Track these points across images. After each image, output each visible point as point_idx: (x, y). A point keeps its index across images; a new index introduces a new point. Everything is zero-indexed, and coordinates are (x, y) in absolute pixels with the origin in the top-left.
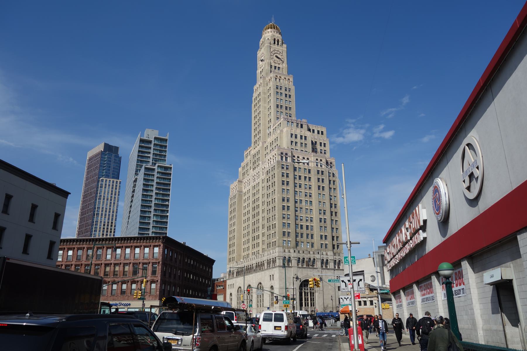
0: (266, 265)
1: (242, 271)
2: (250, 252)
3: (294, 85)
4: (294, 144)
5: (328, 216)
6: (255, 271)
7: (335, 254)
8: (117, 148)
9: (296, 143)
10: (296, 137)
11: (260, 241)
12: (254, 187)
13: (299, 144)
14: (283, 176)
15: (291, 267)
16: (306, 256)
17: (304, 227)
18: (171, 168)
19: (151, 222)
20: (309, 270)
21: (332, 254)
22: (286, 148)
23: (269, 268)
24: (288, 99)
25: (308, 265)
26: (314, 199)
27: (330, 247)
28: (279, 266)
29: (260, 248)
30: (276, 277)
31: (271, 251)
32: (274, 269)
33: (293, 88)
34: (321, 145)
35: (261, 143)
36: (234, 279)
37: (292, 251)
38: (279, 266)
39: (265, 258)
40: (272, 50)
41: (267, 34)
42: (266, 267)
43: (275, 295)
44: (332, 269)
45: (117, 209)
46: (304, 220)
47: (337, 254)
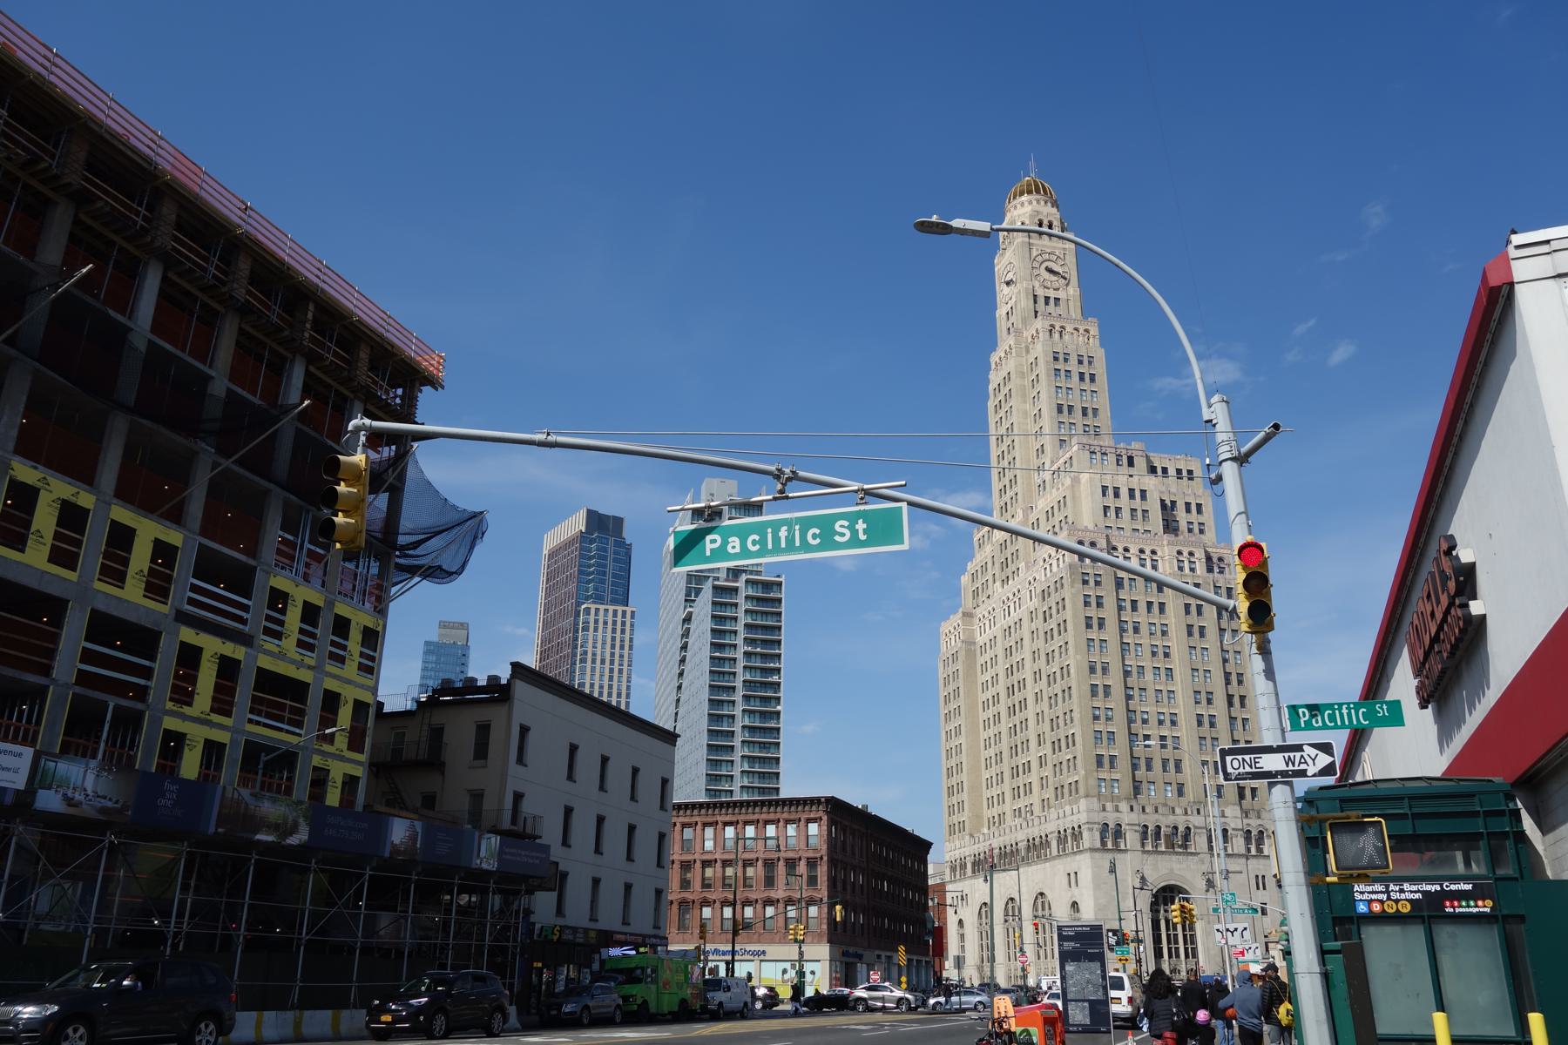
0: (1054, 844)
2: (1008, 807)
3: (1102, 345)
4: (1112, 513)
5: (1219, 708)
6: (1026, 861)
7: (1246, 814)
8: (619, 522)
9: (1118, 510)
10: (1117, 495)
11: (1034, 778)
12: (1008, 631)
13: (1126, 514)
14: (1087, 604)
15: (1125, 851)
16: (1166, 821)
18: (780, 584)
19: (737, 728)
20: (1174, 858)
22: (1091, 527)
24: (1087, 385)
25: (1171, 845)
26: (1178, 663)
28: (1092, 850)
29: (1035, 799)
30: (1086, 876)
32: (1078, 857)
33: (1099, 354)
34: (1188, 510)
35: (1020, 512)
36: (967, 882)
37: (1124, 806)
38: (1092, 850)
39: (1051, 827)
40: (1034, 253)
41: (1020, 211)
42: (1055, 852)
45: (628, 688)
46: (1153, 721)
47: (1252, 814)
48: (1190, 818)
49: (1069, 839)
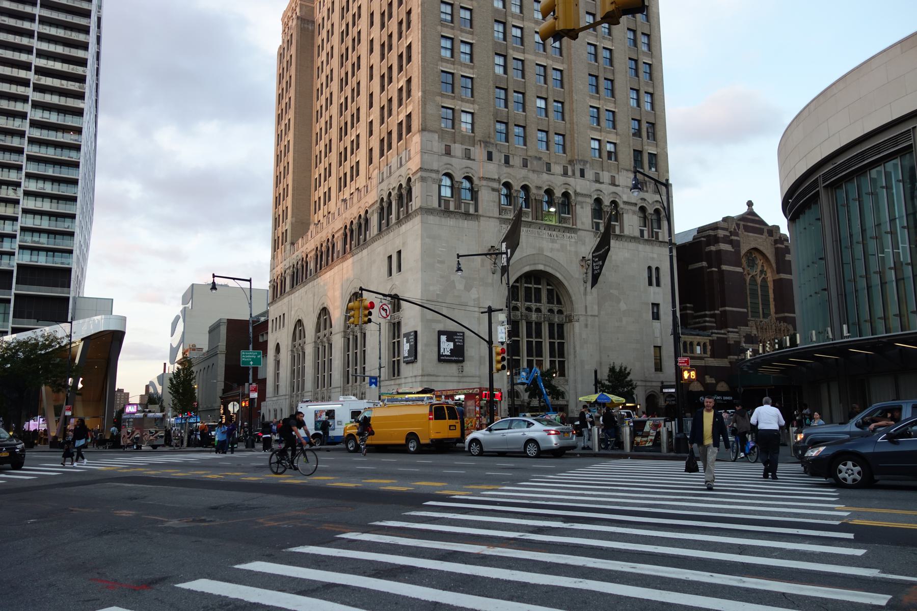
1: (304, 263)
11: (362, 155)
15: (476, 217)
16: (538, 181)
17: (531, 70)
20: (545, 233)
23: (385, 226)
27: (626, 158)
28: (426, 211)
29: (361, 181)
30: (411, 258)
36: (286, 300)
37: (479, 152)
38: (426, 211)
39: (372, 198)
43: (404, 330)
44: (632, 239)
48: (571, 181)
49: (395, 206)
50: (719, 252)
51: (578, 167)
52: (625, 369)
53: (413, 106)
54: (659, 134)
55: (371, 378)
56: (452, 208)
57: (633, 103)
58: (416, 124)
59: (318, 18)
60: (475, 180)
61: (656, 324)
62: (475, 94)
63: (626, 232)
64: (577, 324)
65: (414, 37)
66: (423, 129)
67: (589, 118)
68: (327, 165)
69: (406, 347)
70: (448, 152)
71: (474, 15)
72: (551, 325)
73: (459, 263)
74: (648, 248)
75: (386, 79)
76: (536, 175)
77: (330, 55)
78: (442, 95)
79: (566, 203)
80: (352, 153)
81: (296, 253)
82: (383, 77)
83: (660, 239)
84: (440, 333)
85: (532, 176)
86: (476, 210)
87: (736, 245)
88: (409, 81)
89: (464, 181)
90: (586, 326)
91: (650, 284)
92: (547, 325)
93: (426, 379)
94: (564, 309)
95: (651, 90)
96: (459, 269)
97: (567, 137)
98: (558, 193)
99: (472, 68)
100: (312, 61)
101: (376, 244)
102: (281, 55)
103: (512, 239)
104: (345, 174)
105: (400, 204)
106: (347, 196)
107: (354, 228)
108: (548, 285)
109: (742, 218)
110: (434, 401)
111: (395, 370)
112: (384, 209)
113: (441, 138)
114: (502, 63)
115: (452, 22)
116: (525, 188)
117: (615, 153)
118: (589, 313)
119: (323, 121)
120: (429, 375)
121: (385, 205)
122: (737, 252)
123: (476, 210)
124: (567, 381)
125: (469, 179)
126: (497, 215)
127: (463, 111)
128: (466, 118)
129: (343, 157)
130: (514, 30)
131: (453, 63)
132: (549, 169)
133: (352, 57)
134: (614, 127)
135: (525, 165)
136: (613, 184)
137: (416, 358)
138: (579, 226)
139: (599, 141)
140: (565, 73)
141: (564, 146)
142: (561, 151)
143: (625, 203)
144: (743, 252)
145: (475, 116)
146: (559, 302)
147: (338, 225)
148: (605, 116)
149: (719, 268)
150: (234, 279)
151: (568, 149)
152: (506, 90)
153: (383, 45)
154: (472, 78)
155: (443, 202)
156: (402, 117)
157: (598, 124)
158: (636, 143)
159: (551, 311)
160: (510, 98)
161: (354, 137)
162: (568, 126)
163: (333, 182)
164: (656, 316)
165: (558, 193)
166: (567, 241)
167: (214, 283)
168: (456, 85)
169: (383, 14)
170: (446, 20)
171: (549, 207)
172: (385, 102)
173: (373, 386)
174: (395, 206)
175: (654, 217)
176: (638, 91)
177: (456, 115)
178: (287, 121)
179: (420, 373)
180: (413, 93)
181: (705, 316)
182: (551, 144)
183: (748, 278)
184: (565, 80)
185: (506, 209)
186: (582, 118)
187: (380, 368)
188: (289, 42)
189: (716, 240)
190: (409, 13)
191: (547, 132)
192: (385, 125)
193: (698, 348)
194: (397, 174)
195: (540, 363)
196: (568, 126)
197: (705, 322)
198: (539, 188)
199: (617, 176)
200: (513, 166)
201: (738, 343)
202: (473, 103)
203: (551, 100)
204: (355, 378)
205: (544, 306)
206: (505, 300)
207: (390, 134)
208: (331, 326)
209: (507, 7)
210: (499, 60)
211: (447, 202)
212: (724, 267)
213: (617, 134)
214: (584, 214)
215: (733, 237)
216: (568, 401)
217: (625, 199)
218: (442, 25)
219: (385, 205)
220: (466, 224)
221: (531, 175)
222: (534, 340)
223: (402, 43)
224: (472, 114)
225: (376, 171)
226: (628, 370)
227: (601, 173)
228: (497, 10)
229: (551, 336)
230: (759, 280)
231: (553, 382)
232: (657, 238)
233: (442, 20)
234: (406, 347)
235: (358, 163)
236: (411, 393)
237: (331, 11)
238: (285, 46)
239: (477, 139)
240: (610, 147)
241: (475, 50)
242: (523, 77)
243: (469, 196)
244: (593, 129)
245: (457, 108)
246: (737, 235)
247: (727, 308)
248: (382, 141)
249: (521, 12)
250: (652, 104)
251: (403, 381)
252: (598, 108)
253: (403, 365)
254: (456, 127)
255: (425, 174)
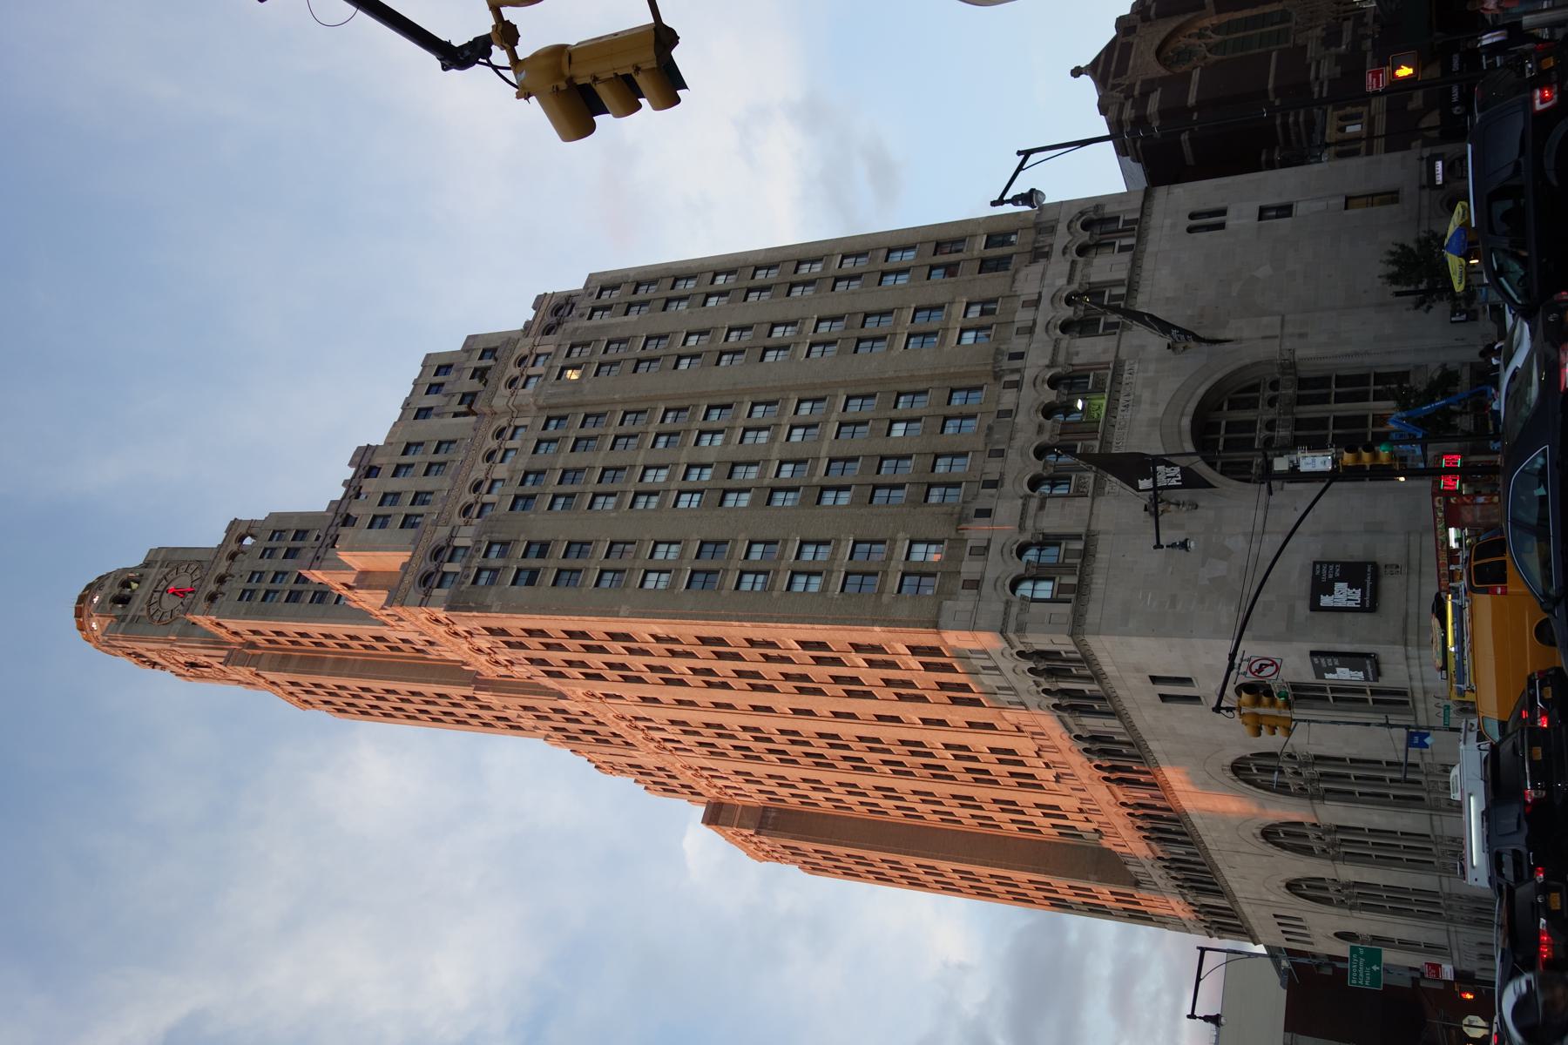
0: (1094, 724)
1: (1172, 864)
7: (1039, 254)
11: (980, 742)
15: (1089, 538)
16: (1028, 429)
17: (846, 448)
20: (1122, 415)
21: (1037, 268)
22: (404, 557)
27: (991, 285)
28: (1077, 627)
29: (1024, 746)
30: (1163, 655)
31: (990, 681)
32: (1108, 669)
36: (1247, 909)
37: (977, 532)
38: (1077, 627)
43: (1309, 677)
44: (1135, 265)
48: (1029, 374)
50: (1162, 113)
51: (1006, 364)
52: (1392, 253)
53: (897, 641)
54: (955, 233)
55: (1410, 743)
56: (1073, 580)
57: (902, 280)
58: (926, 638)
59: (759, 800)
60: (1026, 537)
61: (1300, 209)
62: (880, 537)
63: (1122, 274)
64: (1299, 353)
65: (788, 635)
66: (935, 625)
67: (924, 350)
68: (996, 807)
69: (1344, 674)
70: (974, 585)
71: (759, 538)
72: (1301, 400)
73: (1173, 546)
74: (1153, 236)
75: (853, 688)
76: (1018, 435)
77: (816, 785)
78: (881, 592)
79: (1068, 381)
80: (975, 759)
81: (1155, 879)
82: (850, 694)
83: (1137, 216)
84: (1315, 606)
85: (1018, 442)
86: (1078, 537)
87: (1149, 86)
88: (857, 648)
89: (1025, 558)
90: (1301, 336)
91: (1221, 226)
92: (1301, 408)
93: (1412, 638)
94: (1269, 379)
95: (883, 253)
96: (1184, 545)
97: (956, 384)
98: (1050, 396)
99: (839, 541)
100: (825, 816)
101: (1138, 724)
102: (815, 869)
103: (1133, 468)
104: (1012, 774)
105: (1064, 674)
106: (1049, 775)
107: (1107, 764)
108: (1220, 408)
109: (1101, 83)
110: (1463, 584)
111: (1394, 700)
112: (1071, 705)
113: (951, 595)
114: (833, 494)
115: (766, 573)
116: (1040, 452)
117: (983, 303)
118: (1278, 332)
119: (921, 808)
120: (1405, 631)
121: (1065, 702)
122: (1162, 81)
123: (1078, 537)
124: (1418, 367)
125: (1021, 550)
126: (1087, 501)
127: (908, 557)
128: (919, 550)
129: (982, 777)
130: (782, 475)
131: (830, 572)
132: (1008, 413)
133: (820, 746)
134: (941, 307)
135: (1000, 453)
136: (1036, 303)
137: (1367, 655)
138: (1110, 357)
139: (962, 331)
140: (852, 391)
141: (970, 389)
142: (978, 394)
143: (1070, 281)
144: (1163, 72)
145: (917, 537)
146: (1255, 388)
147: (1102, 794)
148: (922, 323)
149: (1191, 110)
150: (1198, 980)
151: (975, 382)
152: (876, 487)
153: (801, 690)
154: (855, 543)
155: (1061, 596)
156: (914, 662)
157: (935, 334)
158: (968, 272)
159: (1271, 402)
160: (887, 481)
161: (948, 754)
162: (936, 384)
163: (1025, 798)
164: (1285, 210)
165: (1050, 396)
166: (1136, 378)
167: (1206, 1019)
168: (864, 568)
169: (754, 688)
170: (765, 583)
171: (1076, 411)
172: (890, 692)
173: (1428, 740)
174: (1070, 685)
175: (1097, 230)
176: (884, 274)
177: (913, 569)
178: (921, 870)
179: (1399, 649)
180: (875, 642)
181: (1285, 125)
182: (965, 411)
183: (1212, 58)
184: (862, 390)
185: (1077, 486)
186: (926, 359)
187: (1388, 725)
188: (795, 852)
189: (1141, 121)
190: (752, 643)
191: (946, 419)
192: (928, 694)
193: (1349, 129)
194: (1011, 676)
195: (1381, 419)
196: (936, 384)
197: (1296, 122)
198: (1040, 429)
199: (1023, 298)
200: (1002, 475)
201: (1340, 59)
202: (894, 541)
203: (893, 414)
204: (1413, 784)
205: (1263, 414)
206: (1250, 486)
207: (942, 686)
208: (1301, 824)
209: (747, 485)
210: (829, 498)
211: (1062, 588)
212: (1191, 100)
213: (952, 303)
214: (1090, 350)
215: (1136, 93)
216: (1463, 364)
217: (1064, 281)
218: (772, 589)
219: (1065, 702)
220: (1102, 556)
221: (1017, 443)
222: (1331, 432)
223: (797, 656)
224: (912, 542)
225: (1006, 714)
226: (1394, 249)
227: (1017, 325)
228: (752, 503)
229: (1324, 399)
230: (1217, 38)
231: (1422, 388)
232: (1135, 221)
233: (764, 589)
234: (1344, 674)
235: (993, 750)
236: (1445, 639)
237: (748, 777)
238: (800, 859)
239: (953, 535)
240: (976, 309)
241: (811, 536)
242: (855, 459)
243: (1053, 551)
244: (942, 343)
245: (901, 567)
246: (1132, 86)
247: (1270, 86)
248: (954, 701)
249: (755, 464)
250: (905, 249)
251: (1417, 684)
252: (910, 336)
253: (1383, 683)
254: (932, 569)
255: (1012, 625)
